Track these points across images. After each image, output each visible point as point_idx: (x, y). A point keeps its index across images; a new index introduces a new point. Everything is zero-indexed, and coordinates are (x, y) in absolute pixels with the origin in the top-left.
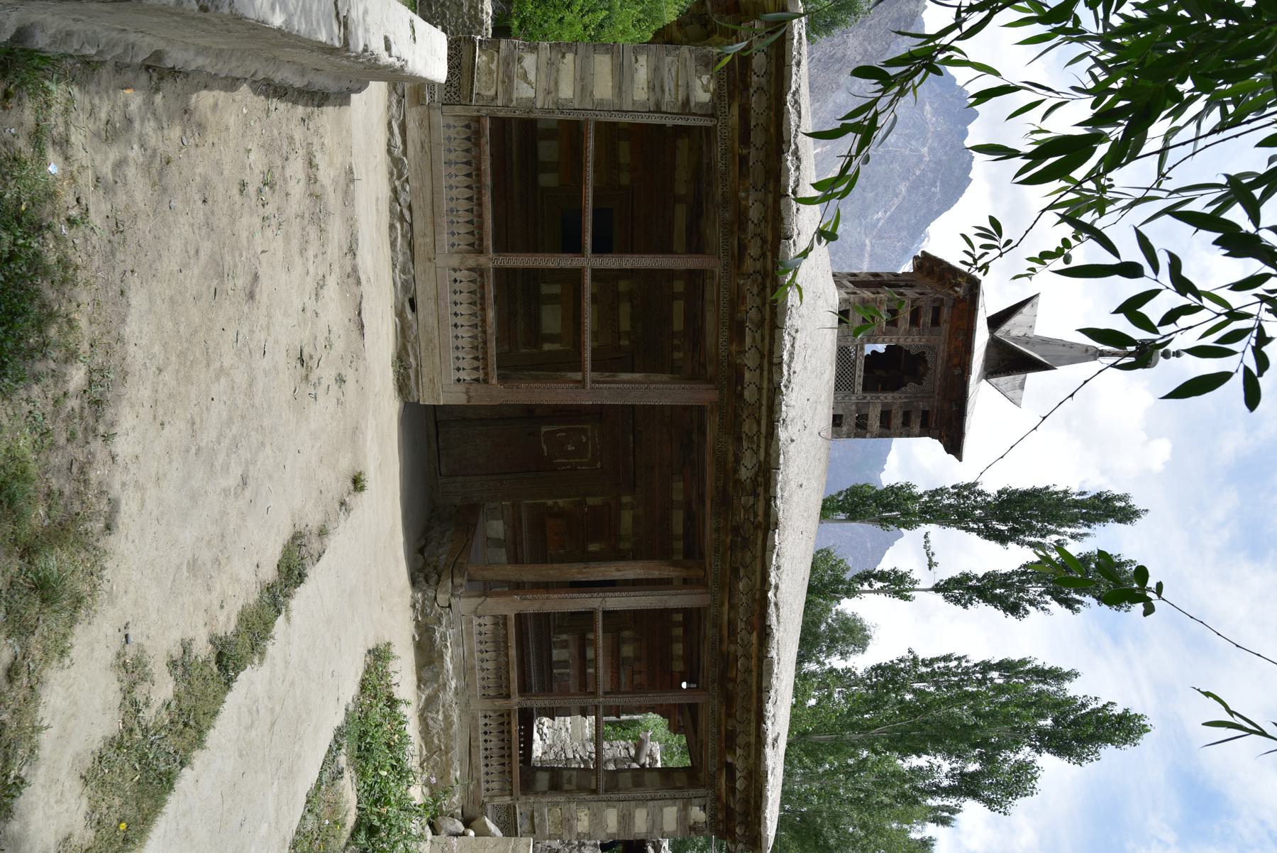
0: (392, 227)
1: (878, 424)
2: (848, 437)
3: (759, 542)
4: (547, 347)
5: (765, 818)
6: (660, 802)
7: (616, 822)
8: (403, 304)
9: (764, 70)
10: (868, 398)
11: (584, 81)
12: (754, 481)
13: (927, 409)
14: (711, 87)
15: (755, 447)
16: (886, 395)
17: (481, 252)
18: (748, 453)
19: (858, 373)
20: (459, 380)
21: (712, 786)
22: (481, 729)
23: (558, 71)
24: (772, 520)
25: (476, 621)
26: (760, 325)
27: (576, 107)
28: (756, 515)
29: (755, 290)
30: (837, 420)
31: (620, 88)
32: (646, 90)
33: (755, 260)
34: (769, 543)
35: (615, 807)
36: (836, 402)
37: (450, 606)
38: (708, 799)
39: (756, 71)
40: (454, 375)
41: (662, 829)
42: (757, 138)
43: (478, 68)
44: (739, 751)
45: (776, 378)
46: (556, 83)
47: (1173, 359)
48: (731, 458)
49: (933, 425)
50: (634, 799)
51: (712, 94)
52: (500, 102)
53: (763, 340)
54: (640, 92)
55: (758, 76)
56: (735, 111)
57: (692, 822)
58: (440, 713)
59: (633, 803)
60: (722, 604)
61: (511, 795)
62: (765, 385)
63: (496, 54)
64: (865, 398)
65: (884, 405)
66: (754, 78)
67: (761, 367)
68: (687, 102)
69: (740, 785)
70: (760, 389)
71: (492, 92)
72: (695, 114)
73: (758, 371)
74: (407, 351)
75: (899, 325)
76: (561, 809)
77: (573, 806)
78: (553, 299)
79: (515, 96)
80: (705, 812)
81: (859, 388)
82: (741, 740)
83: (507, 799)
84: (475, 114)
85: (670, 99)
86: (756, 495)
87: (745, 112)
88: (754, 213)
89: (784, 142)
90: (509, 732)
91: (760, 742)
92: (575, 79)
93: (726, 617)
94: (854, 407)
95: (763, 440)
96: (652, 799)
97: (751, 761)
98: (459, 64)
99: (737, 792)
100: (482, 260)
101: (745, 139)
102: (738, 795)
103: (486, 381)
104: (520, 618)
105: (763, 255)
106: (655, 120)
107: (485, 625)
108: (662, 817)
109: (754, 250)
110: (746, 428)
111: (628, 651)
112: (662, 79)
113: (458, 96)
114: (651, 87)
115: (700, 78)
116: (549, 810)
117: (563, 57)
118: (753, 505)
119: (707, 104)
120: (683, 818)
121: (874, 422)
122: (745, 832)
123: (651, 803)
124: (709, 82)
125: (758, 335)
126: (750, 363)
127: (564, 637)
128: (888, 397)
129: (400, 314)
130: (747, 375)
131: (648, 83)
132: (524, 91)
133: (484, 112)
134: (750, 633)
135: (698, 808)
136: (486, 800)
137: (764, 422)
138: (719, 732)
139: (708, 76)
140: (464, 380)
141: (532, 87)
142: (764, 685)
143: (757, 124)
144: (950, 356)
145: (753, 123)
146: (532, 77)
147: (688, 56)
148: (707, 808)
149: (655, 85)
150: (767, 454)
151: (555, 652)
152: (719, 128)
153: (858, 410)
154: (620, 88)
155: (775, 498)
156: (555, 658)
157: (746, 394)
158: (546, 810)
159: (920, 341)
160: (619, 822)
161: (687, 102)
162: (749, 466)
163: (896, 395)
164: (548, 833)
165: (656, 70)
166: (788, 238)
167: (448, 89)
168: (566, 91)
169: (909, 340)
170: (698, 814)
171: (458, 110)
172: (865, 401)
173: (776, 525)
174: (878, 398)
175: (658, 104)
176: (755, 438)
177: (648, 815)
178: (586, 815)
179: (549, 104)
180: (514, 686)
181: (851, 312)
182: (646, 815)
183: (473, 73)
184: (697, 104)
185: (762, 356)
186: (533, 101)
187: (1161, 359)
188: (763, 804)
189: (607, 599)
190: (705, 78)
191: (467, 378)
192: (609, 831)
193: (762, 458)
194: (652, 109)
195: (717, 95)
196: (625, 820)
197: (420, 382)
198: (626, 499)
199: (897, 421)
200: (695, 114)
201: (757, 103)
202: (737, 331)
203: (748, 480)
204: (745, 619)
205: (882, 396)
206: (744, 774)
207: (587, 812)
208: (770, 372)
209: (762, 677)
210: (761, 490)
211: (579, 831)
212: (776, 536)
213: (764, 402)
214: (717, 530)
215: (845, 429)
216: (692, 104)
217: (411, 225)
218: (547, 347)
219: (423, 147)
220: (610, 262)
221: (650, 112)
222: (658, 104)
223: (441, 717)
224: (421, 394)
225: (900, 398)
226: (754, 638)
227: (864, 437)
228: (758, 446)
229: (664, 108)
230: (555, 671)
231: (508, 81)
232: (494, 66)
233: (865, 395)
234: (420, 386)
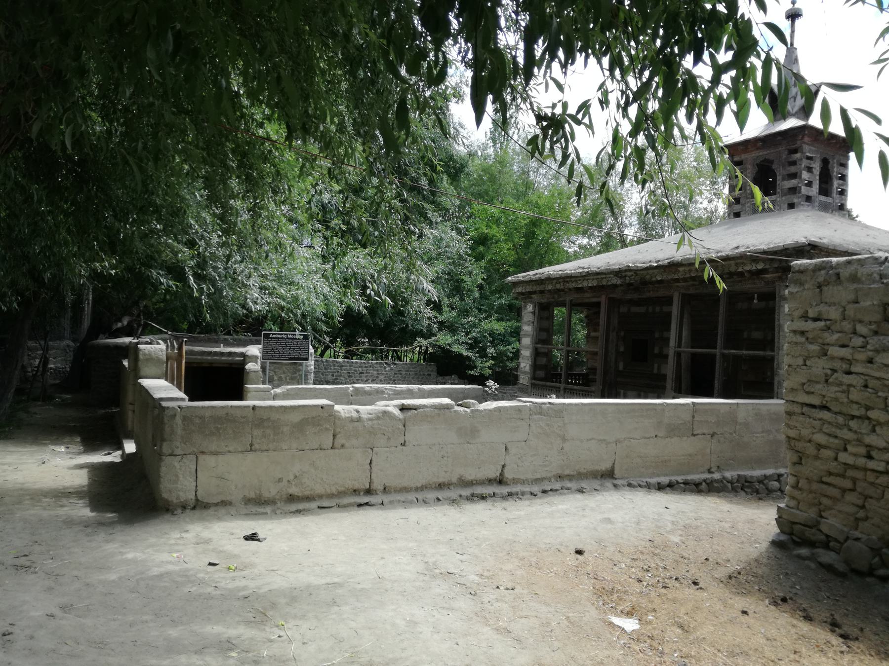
1: (793, 181)
3: (641, 272)
12: (621, 277)
13: (786, 153)
17: (559, 388)
21: (773, 282)
26: (576, 281)
28: (632, 275)
38: (781, 284)
44: (740, 269)
48: (622, 288)
50: (779, 333)
56: (533, 296)
59: (781, 333)
60: (677, 286)
62: (592, 277)
65: (783, 179)
67: (587, 280)
70: (593, 279)
78: (659, 368)
82: (733, 269)
86: (626, 276)
87: (531, 293)
88: (550, 287)
93: (683, 284)
94: (784, 198)
95: (608, 276)
97: (745, 262)
100: (562, 388)
102: (768, 267)
105: (560, 283)
109: (558, 286)
110: (604, 283)
114: (529, 325)
125: (579, 282)
130: (590, 285)
134: (679, 271)
138: (740, 281)
144: (757, 149)
153: (785, 195)
163: (778, 174)
179: (530, 359)
193: (612, 276)
195: (531, 302)
198: (745, 335)
201: (529, 289)
205: (778, 182)
206: (754, 265)
208: (585, 276)
210: (623, 274)
213: (596, 277)
214: (649, 292)
226: (681, 269)
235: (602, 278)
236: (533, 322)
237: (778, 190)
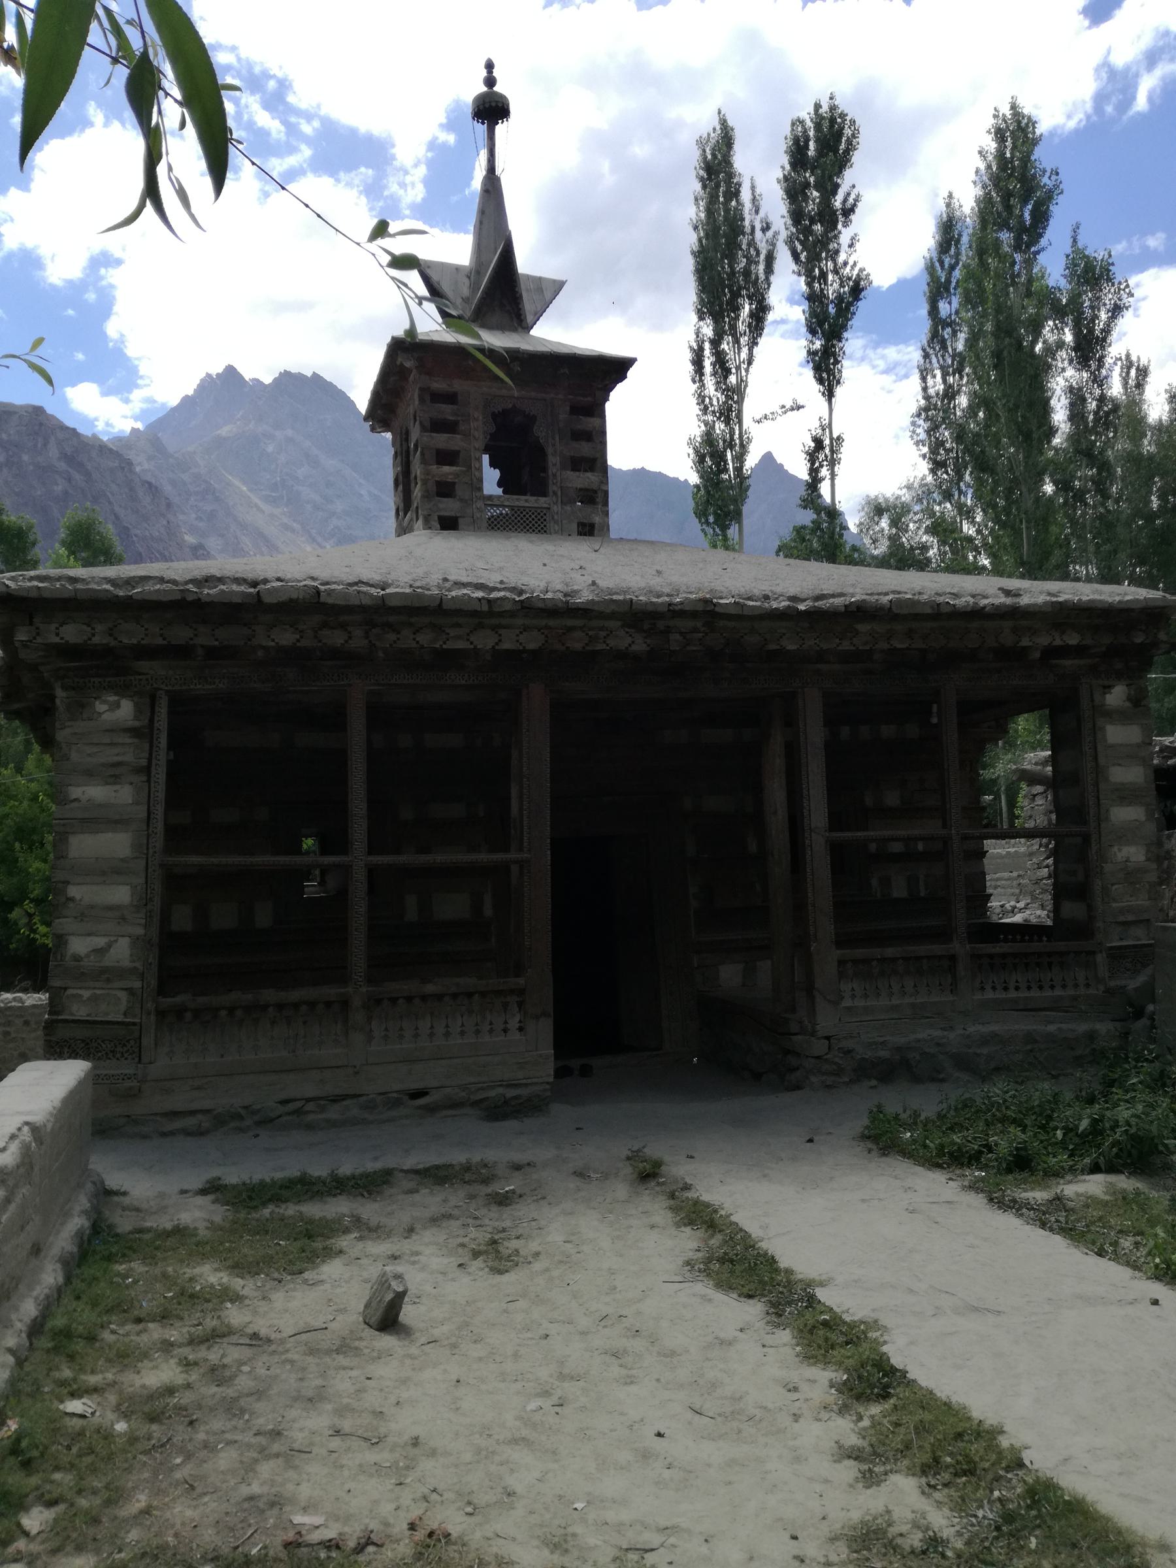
0: (310, 1127)
1: (589, 474)
2: (607, 514)
4: (488, 911)
5: (1120, 602)
6: (1100, 748)
7: (1130, 808)
8: (419, 1107)
9: (85, 627)
10: (555, 488)
11: (108, 871)
13: (568, 408)
14: (113, 698)
15: (603, 634)
16: (550, 464)
17: (345, 1004)
18: (612, 643)
19: (522, 503)
20: (521, 1029)
22: (1000, 995)
23: (92, 907)
24: (700, 607)
25: (847, 1002)
27: (142, 880)
28: (695, 630)
29: (392, 637)
30: (587, 530)
31: (117, 822)
32: (117, 787)
33: (350, 638)
34: (733, 612)
35: (1108, 811)
36: (563, 532)
37: (828, 1038)
39: (85, 638)
40: (515, 1036)
41: (1138, 746)
42: (181, 634)
43: (88, 1015)
45: (508, 607)
46: (110, 908)
47: (496, 73)
49: (589, 399)
50: (1096, 784)
51: (123, 697)
52: (137, 984)
53: (459, 625)
54: (122, 795)
55: (93, 635)
56: (144, 665)
57: (1128, 704)
58: (978, 1051)
61: (1094, 953)
63: (69, 992)
64: (555, 493)
66: (96, 640)
68: (134, 732)
69: (1073, 639)
70: (526, 629)
71: (123, 995)
72: (151, 721)
73: (502, 631)
74: (481, 1101)
75: (457, 448)
76: (1113, 885)
77: (1108, 867)
79: (126, 963)
80: (1114, 686)
81: (542, 502)
83: (1100, 958)
84: (153, 1017)
85: (129, 753)
87: (145, 652)
88: (286, 637)
89: (184, 599)
90: (1004, 956)
91: (1014, 615)
92: (104, 883)
94: (568, 508)
96: (1096, 758)
98: (83, 1041)
99: (1084, 642)
101: (181, 652)
102: (1088, 641)
103: (521, 992)
104: (839, 944)
105: (343, 626)
106: (160, 774)
107: (853, 989)
108: (1121, 745)
109: (336, 638)
110: (578, 646)
111: (892, 799)
112: (103, 765)
113: (128, 1041)
114: (115, 779)
115: (100, 714)
116: (1115, 900)
117: (72, 899)
118: (681, 633)
119: (136, 705)
120: (1121, 716)
121: (587, 479)
122: (1141, 630)
123: (1102, 761)
124: (105, 702)
125: (453, 632)
126: (490, 643)
127: (874, 882)
128: (553, 461)
129: (431, 1109)
130: (506, 646)
131: (107, 784)
132: (122, 952)
133: (150, 1005)
135: (1108, 696)
136: (1102, 988)
137: (570, 622)
139: (97, 703)
140: (520, 1022)
141: (116, 941)
142: (929, 611)
143: (161, 635)
145: (160, 641)
146: (100, 942)
147: (67, 731)
148: (1106, 683)
149: (112, 774)
150: (613, 616)
151: (896, 894)
152: (170, 688)
154: (117, 822)
155: (670, 605)
156: (904, 894)
157: (532, 646)
158: (1114, 905)
159: (477, 420)
160: (1130, 804)
161: (134, 732)
162: (629, 640)
163: (550, 450)
164: (1147, 903)
165: (90, 774)
166: (318, 592)
167: (118, 1055)
168: (121, 894)
169: (476, 434)
170: (1116, 696)
171: (148, 1041)
172: (559, 493)
173: (706, 601)
174: (554, 475)
175: (138, 771)
176: (590, 633)
177: (1120, 765)
178: (1120, 850)
180: (937, 949)
181: (443, 513)
182: (1119, 768)
183: (95, 1022)
184: (136, 718)
185: (480, 626)
186: (135, 940)
187: (495, 89)
188: (1100, 606)
189: (813, 826)
190: (100, 707)
191: (517, 1018)
192: (1143, 818)
194: (145, 778)
195: (123, 690)
196: (1127, 795)
197: (525, 1081)
199: (585, 449)
200: (151, 721)
201: (132, 634)
202: (447, 659)
203: (648, 641)
204: (837, 641)
205: (552, 470)
207: (1115, 849)
208: (501, 614)
209: (917, 615)
210: (661, 624)
211: (1142, 858)
212: (722, 601)
215: (597, 520)
216: (137, 724)
217: (308, 1100)
218: (488, 911)
219: (199, 1088)
220: (359, 830)
221: (149, 781)
222: (138, 771)
223: (985, 1051)
224: (541, 1080)
225: (554, 445)
226: (863, 628)
227: (606, 493)
228: (602, 629)
229: (144, 762)
230: (922, 894)
231: (107, 975)
232: (86, 994)
233: (551, 493)
234: (529, 1081)
235: (571, 629)
236: (147, 770)
237: (552, 488)
